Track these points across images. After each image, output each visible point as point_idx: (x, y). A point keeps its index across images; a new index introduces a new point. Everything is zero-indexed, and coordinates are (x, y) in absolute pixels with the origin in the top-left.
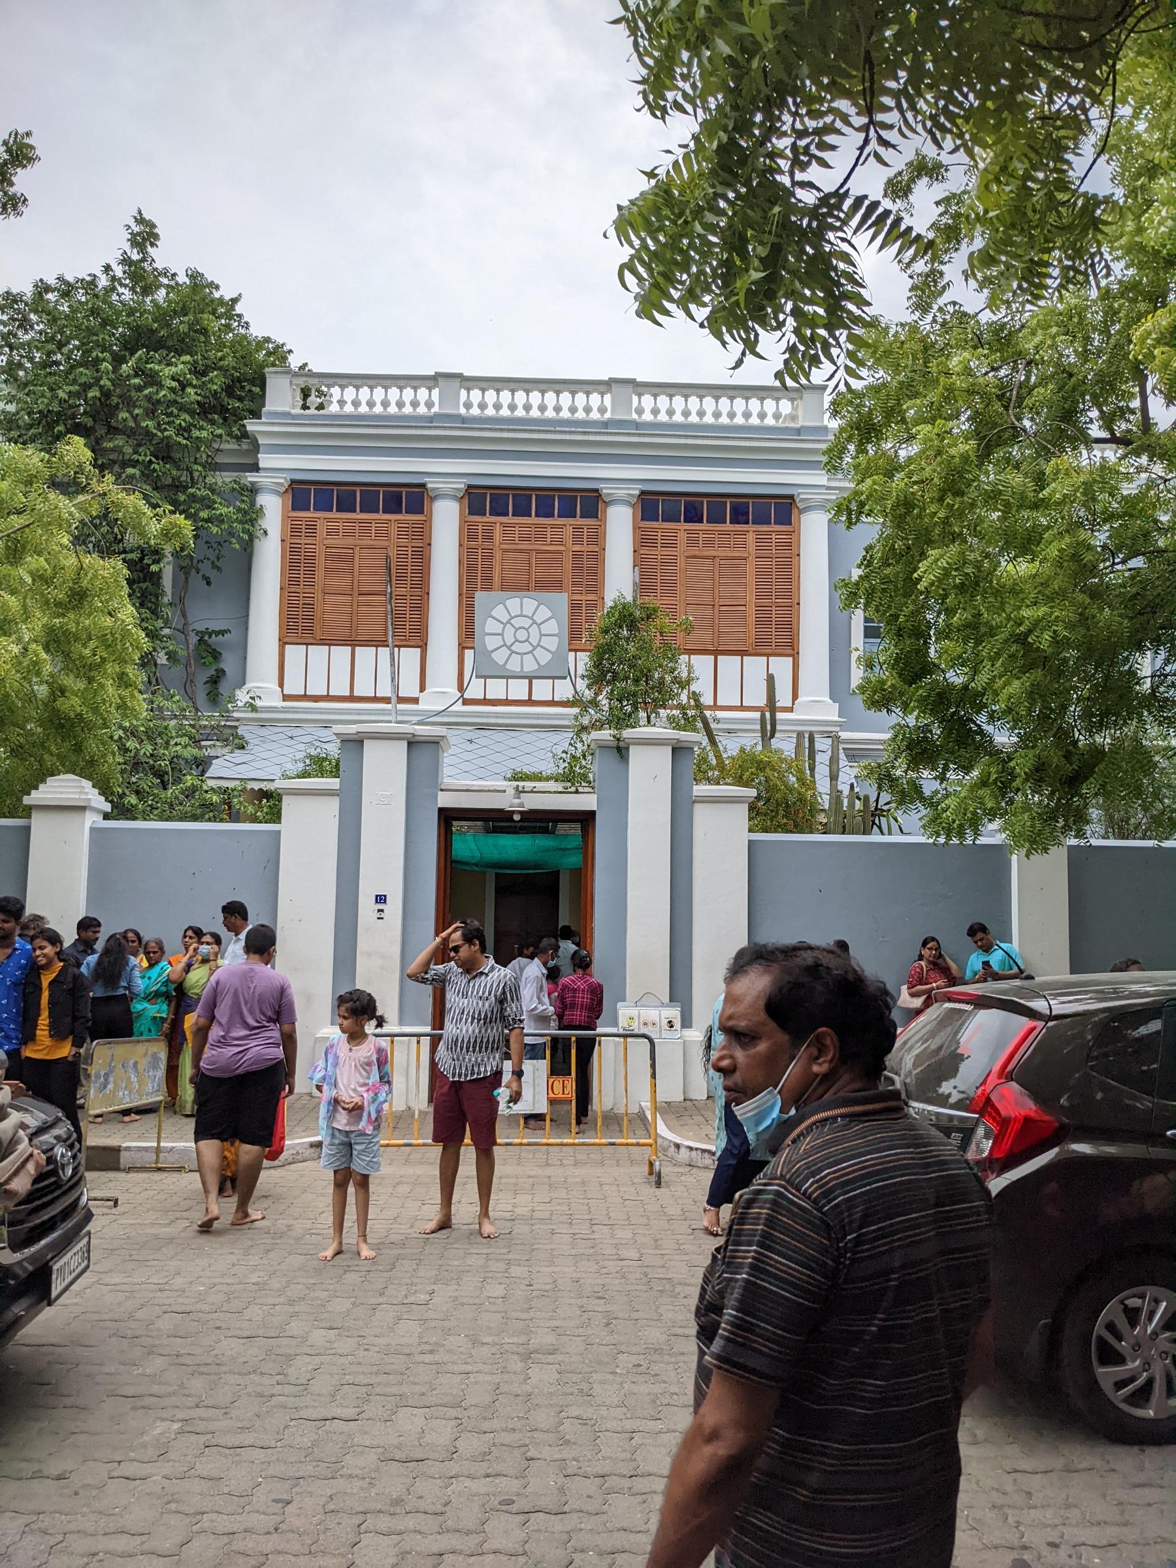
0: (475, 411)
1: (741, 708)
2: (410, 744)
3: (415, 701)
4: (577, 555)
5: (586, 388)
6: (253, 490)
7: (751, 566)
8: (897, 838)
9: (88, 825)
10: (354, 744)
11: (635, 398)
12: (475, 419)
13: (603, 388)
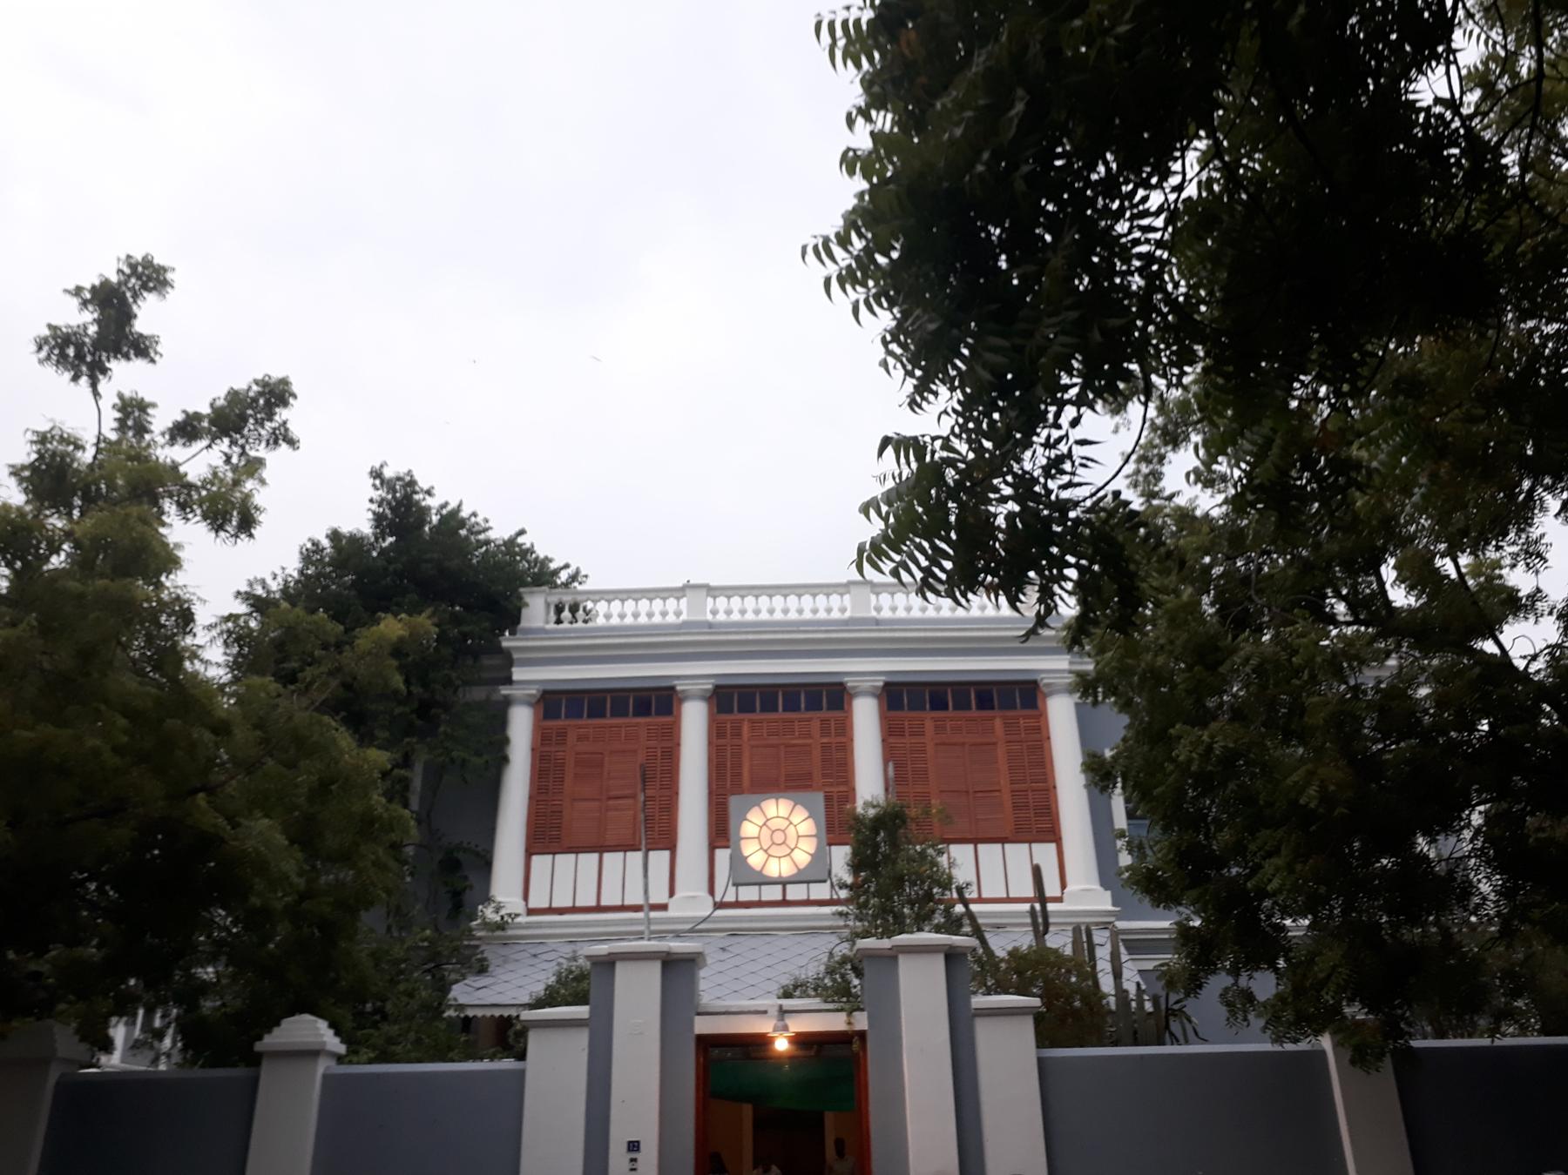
0: (721, 617)
1: (1008, 900)
3: (664, 907)
4: (825, 747)
6: (507, 702)
7: (1001, 751)
10: (607, 964)
11: (873, 597)
12: (721, 625)
13: (841, 590)
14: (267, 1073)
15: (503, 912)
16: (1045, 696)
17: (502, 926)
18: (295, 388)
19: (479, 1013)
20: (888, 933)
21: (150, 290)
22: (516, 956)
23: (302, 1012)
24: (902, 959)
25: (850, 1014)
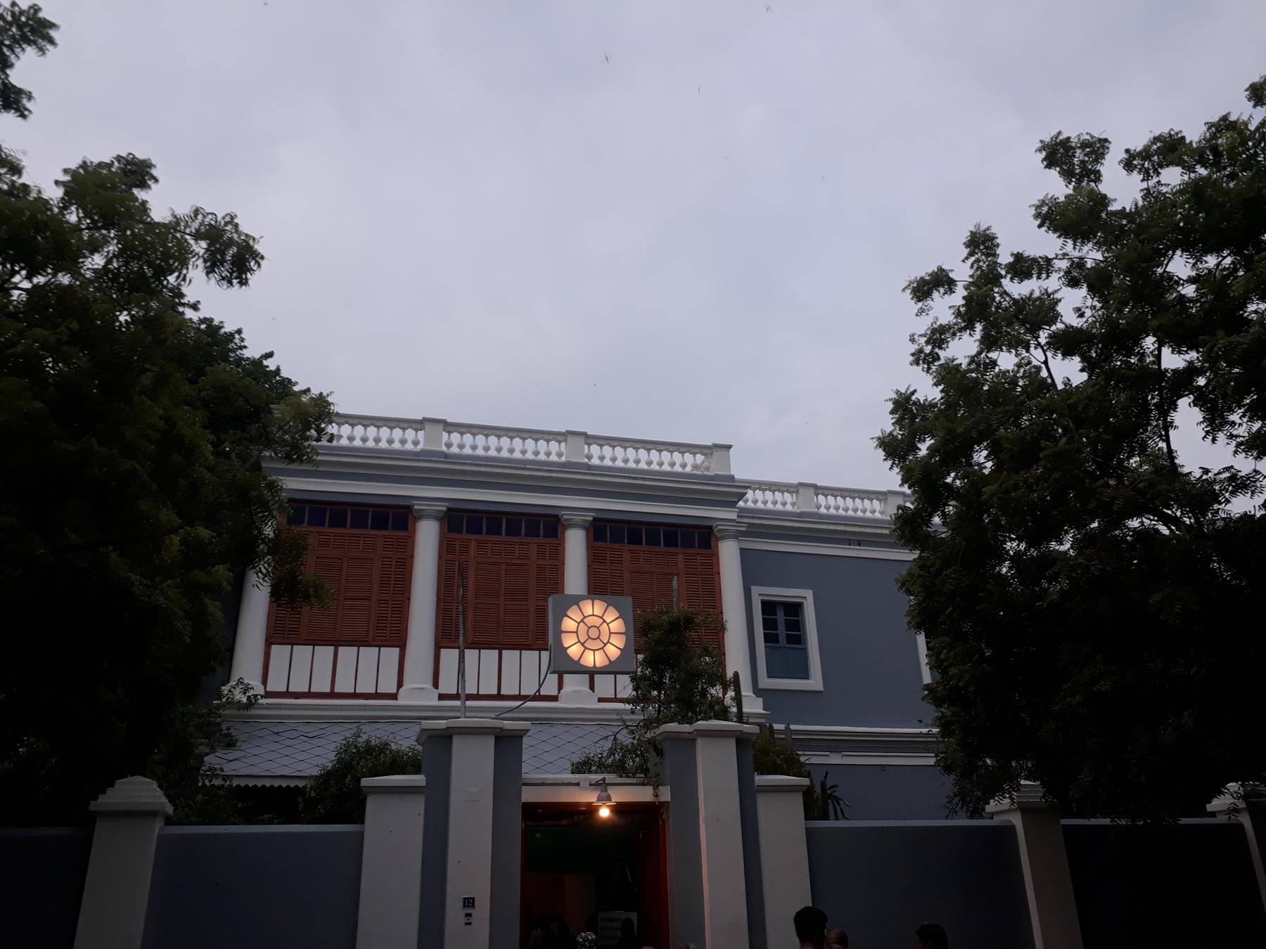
2: (497, 739)
3: (394, 696)
5: (547, 437)
13: (560, 438)
14: (102, 832)
15: (251, 693)
16: (718, 539)
17: (252, 702)
18: (154, 172)
21: (29, 42)
24: (699, 741)
25: (656, 787)
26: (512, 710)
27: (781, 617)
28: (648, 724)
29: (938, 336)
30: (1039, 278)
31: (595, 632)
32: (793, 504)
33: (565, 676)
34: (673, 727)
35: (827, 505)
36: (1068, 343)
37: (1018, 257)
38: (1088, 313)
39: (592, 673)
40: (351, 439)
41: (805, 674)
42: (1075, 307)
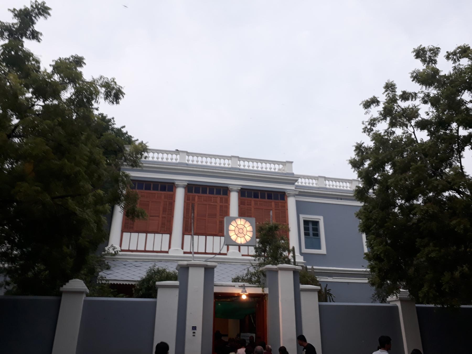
8: (332, 303)
9: (83, 299)
13: (229, 158)
14: (64, 298)
15: (116, 250)
16: (287, 197)
17: (116, 254)
18: (84, 61)
19: (110, 282)
20: (276, 265)
21: (41, 15)
22: (118, 265)
23: (72, 279)
24: (280, 272)
25: (263, 288)
26: (211, 258)
27: (311, 226)
28: (260, 265)
29: (373, 122)
30: (412, 100)
31: (241, 230)
32: (316, 184)
33: (230, 247)
34: (270, 266)
35: (329, 185)
36: (422, 125)
37: (404, 93)
38: (431, 114)
39: (239, 246)
40: (153, 158)
41: (319, 247)
42: (426, 111)
